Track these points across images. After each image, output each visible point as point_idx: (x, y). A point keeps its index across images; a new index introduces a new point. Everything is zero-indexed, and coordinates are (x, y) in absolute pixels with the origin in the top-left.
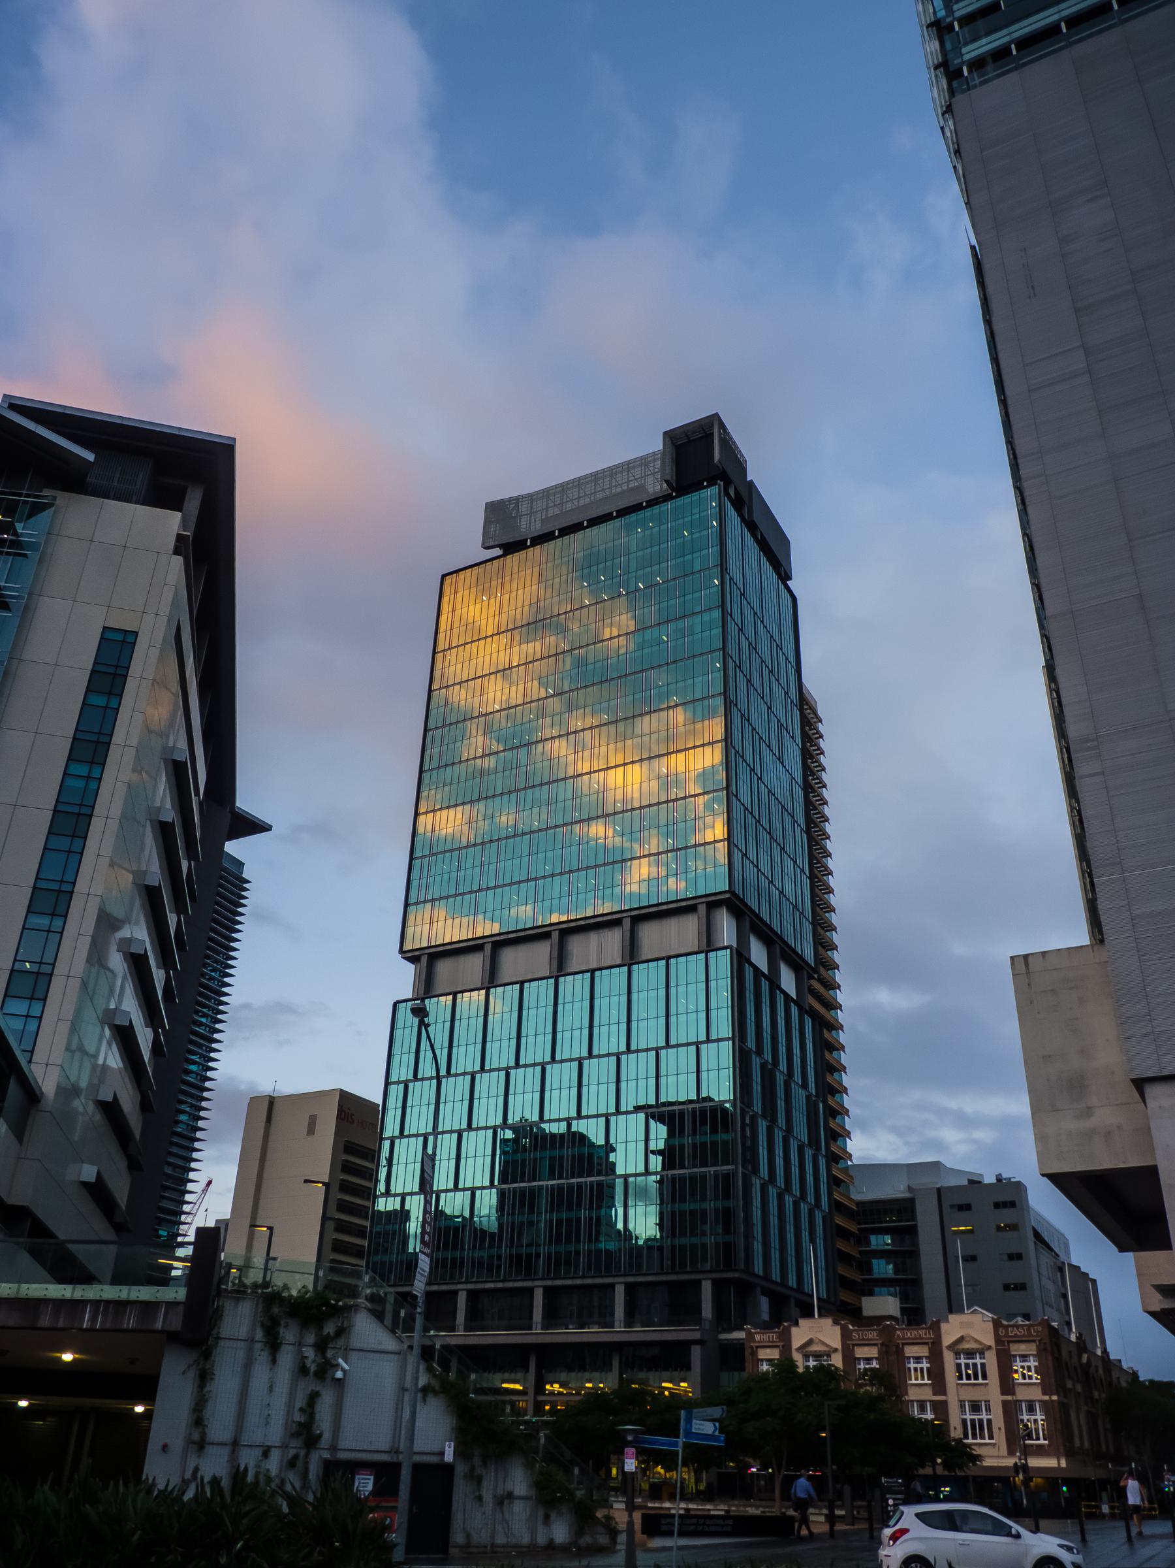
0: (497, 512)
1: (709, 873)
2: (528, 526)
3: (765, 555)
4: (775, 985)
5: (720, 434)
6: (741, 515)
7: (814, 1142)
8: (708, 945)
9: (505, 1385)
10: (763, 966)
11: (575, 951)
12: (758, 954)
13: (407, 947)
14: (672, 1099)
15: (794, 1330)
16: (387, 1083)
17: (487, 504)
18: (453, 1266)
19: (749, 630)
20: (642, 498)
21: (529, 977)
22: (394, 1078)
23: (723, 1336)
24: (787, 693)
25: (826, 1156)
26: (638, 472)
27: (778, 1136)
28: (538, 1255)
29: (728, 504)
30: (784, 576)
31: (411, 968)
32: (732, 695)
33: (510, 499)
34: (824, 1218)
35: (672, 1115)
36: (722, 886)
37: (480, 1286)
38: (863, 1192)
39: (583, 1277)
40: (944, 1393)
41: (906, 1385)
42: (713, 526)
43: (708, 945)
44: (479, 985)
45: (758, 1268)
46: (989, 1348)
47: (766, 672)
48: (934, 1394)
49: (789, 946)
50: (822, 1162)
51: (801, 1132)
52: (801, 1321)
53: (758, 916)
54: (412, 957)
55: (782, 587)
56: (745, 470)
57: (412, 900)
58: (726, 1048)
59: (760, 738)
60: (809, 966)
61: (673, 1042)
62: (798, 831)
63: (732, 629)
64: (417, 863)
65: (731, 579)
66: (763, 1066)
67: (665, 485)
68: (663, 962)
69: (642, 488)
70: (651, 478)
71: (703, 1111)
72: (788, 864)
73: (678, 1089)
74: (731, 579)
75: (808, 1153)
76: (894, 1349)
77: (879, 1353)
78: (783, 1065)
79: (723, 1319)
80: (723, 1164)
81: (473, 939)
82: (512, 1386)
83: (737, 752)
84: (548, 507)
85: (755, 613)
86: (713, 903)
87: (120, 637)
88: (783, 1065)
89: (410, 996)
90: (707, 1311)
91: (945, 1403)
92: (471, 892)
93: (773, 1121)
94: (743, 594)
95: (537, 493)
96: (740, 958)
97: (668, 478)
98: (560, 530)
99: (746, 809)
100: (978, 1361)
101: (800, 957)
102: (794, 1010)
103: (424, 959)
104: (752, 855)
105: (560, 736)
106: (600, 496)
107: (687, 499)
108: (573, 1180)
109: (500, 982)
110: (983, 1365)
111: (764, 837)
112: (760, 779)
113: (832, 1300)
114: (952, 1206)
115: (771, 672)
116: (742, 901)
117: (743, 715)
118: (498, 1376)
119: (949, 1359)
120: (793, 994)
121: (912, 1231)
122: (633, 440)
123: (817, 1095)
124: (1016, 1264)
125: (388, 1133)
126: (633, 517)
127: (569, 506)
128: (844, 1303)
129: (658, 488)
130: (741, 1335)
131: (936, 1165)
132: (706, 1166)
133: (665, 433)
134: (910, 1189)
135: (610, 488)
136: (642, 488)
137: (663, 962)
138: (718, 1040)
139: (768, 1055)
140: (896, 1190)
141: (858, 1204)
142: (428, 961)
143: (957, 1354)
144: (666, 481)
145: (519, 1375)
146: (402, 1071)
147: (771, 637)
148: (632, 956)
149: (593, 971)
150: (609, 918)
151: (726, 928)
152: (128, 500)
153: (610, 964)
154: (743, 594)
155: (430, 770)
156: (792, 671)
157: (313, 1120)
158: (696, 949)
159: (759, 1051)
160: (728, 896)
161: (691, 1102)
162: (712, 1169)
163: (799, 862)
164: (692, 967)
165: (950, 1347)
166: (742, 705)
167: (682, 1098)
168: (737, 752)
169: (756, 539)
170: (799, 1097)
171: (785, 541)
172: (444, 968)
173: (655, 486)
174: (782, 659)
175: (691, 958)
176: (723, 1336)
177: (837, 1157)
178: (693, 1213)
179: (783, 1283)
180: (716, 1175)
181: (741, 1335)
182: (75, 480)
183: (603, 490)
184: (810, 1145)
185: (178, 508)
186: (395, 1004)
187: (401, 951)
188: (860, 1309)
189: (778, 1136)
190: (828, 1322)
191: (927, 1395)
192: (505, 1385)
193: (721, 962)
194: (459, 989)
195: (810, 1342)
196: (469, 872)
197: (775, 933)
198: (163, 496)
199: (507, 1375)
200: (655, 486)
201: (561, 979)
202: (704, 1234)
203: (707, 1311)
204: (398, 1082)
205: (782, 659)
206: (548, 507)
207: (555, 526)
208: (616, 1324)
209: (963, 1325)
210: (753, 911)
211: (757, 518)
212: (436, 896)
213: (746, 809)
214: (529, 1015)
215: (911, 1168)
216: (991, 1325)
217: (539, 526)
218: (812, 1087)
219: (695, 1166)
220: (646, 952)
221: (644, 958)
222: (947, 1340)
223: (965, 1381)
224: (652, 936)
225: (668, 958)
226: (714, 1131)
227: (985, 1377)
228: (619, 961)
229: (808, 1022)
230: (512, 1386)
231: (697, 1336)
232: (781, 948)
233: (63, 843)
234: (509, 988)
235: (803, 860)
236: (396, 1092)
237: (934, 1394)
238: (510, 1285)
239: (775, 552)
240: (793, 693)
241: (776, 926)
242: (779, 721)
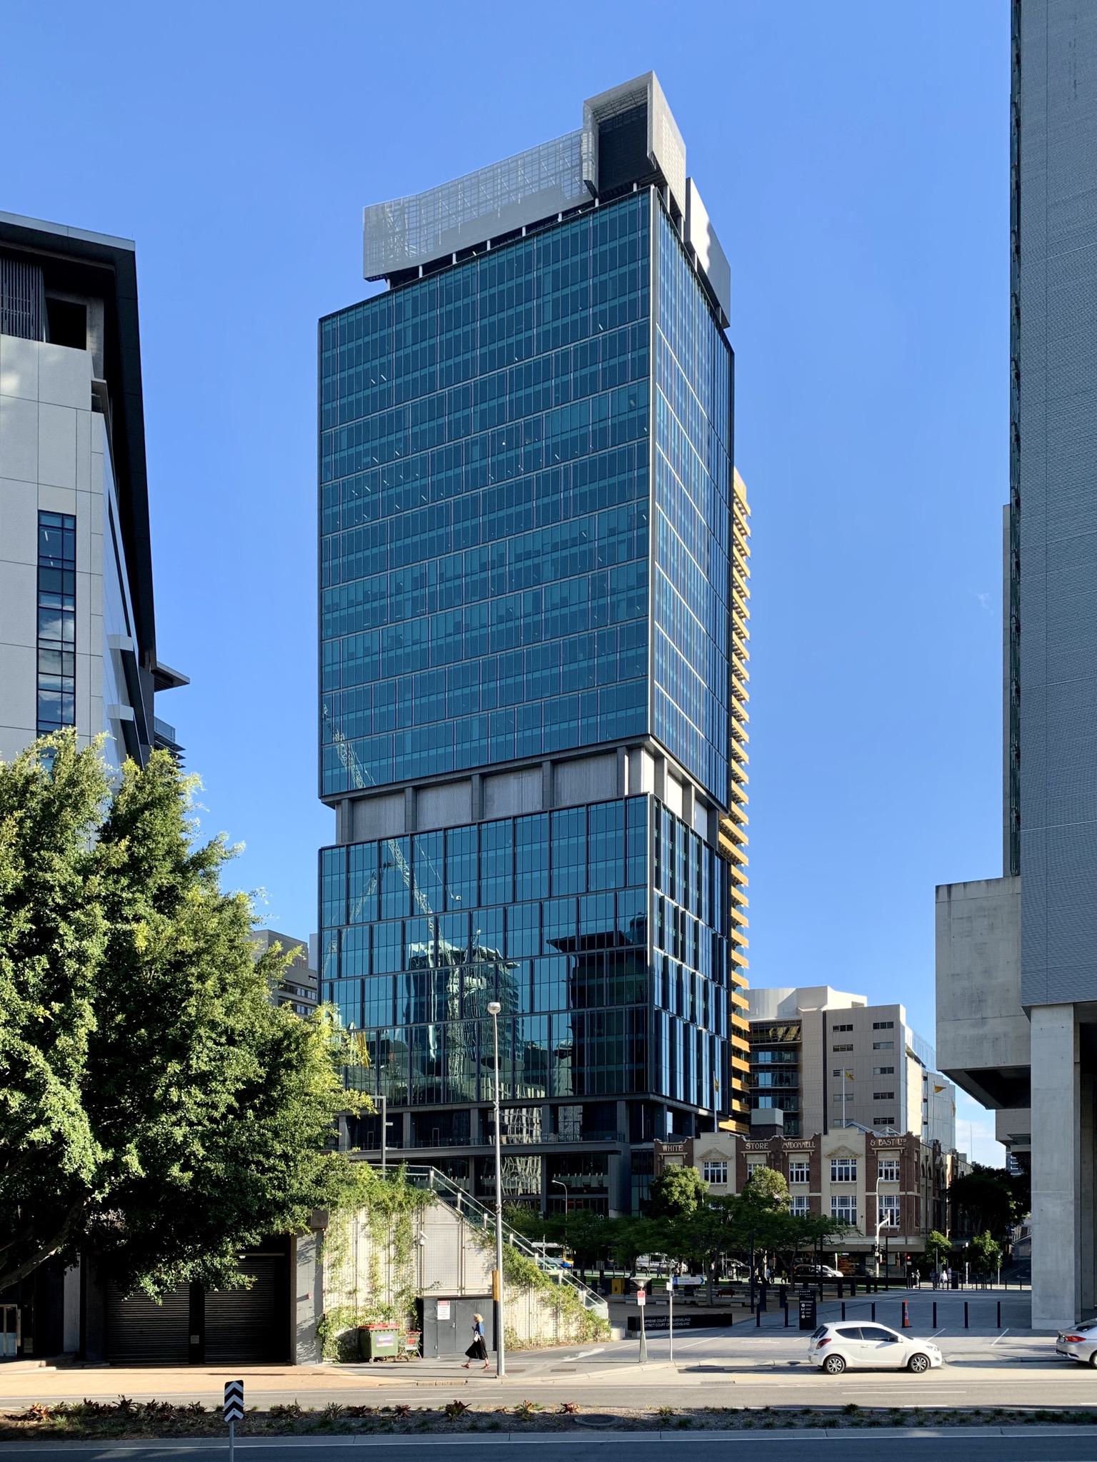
15: (696, 1142)
21: (452, 824)
45: (666, 1091)
50: (723, 993)
52: (702, 1135)
75: (712, 986)
114: (835, 1028)
130: (650, 1145)
172: (366, 811)
181: (650, 1145)
184: (714, 980)
216: (864, 1137)
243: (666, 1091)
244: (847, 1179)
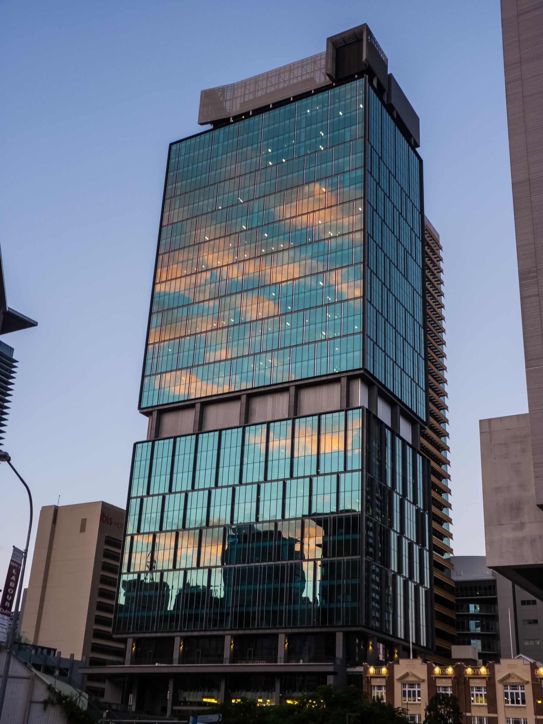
0: (209, 97)
1: (348, 357)
2: (233, 108)
3: (399, 128)
4: (395, 433)
5: (367, 39)
6: (381, 99)
7: (420, 539)
8: (347, 406)
9: (205, 700)
10: (387, 421)
11: (257, 409)
12: (384, 412)
13: (144, 405)
14: (320, 511)
16: (129, 498)
17: (202, 92)
18: (172, 620)
19: (384, 183)
20: (311, 87)
21: (226, 426)
22: (134, 494)
23: (350, 670)
24: (412, 229)
25: (430, 551)
26: (309, 68)
28: (228, 614)
29: (372, 91)
30: (414, 144)
31: (146, 419)
32: (369, 231)
33: (218, 88)
34: (426, 592)
35: (326, 521)
36: (358, 364)
37: (189, 634)
38: (461, 575)
39: (258, 629)
40: (496, 712)
41: (470, 706)
42: (360, 108)
43: (347, 406)
44: (191, 432)
46: (528, 682)
47: (396, 214)
48: (489, 713)
49: (407, 407)
50: (426, 554)
51: (411, 533)
52: (401, 661)
53: (384, 386)
54: (147, 412)
55: (411, 152)
56: (385, 67)
57: (148, 372)
58: (357, 476)
59: (390, 261)
60: (422, 421)
61: (322, 471)
63: (371, 183)
64: (150, 347)
65: (372, 147)
67: (327, 78)
68: (316, 418)
69: (312, 79)
70: (318, 73)
71: (340, 519)
72: (409, 351)
73: (325, 505)
74: (372, 147)
75: (416, 548)
76: (463, 681)
77: (453, 683)
78: (399, 488)
79: (351, 658)
80: (353, 555)
81: (188, 400)
82: (209, 700)
83: (372, 271)
84: (245, 94)
85: (390, 172)
86: (352, 377)
88: (399, 488)
89: (145, 439)
90: (339, 653)
91: (497, 718)
92: (187, 368)
94: (381, 158)
95: (238, 84)
97: (330, 72)
98: (254, 111)
99: (377, 311)
100: (520, 691)
101: (416, 415)
102: (409, 451)
103: (155, 414)
104: (381, 343)
105: (249, 259)
106: (281, 86)
107: (343, 88)
108: (252, 564)
109: (206, 430)
110: (523, 694)
111: (391, 332)
113: (430, 647)
115: (401, 214)
116: (372, 376)
117: (377, 245)
118: (200, 693)
119: (500, 689)
120: (409, 440)
122: (296, 46)
123: (424, 509)
124: (533, 626)
125: (130, 531)
126: (304, 102)
127: (260, 94)
128: (438, 647)
129: (322, 80)
130: (360, 669)
132: (342, 556)
133: (328, 39)
135: (289, 80)
136: (312, 79)
137: (316, 418)
138: (352, 471)
141: (457, 583)
142: (158, 414)
143: (506, 686)
144: (329, 75)
145: (215, 693)
146: (139, 490)
147: (402, 189)
148: (296, 412)
149: (268, 423)
150: (280, 386)
151: (360, 394)
153: (280, 418)
154: (381, 158)
155: (160, 282)
157: (84, 522)
158: (339, 408)
160: (362, 372)
161: (332, 513)
162: (346, 558)
165: (502, 681)
166: (377, 238)
167: (327, 511)
168: (372, 271)
169: (392, 117)
170: (410, 511)
171: (416, 120)
172: (169, 420)
173: (321, 79)
174: (409, 205)
175: (284, 423)
176: (350, 670)
180: (348, 562)
181: (360, 669)
183: (284, 81)
184: (417, 543)
186: (135, 445)
187: (140, 408)
188: (450, 655)
190: (419, 661)
191: (485, 713)
192: (205, 700)
194: (178, 434)
195: (407, 675)
196: (186, 354)
197: (397, 398)
199: (206, 693)
200: (321, 79)
201: (200, 436)
202: (338, 601)
203: (339, 653)
204: (137, 497)
205: (409, 205)
206: (245, 94)
207: (250, 108)
208: (279, 660)
209: (510, 666)
210: (380, 383)
211: (394, 101)
212: (164, 370)
213: (377, 311)
214: (225, 453)
216: (529, 667)
217: (238, 108)
218: (420, 504)
219: (334, 556)
221: (303, 414)
222: (499, 676)
223: (510, 704)
224: (310, 399)
225: (320, 415)
226: (347, 533)
227: (524, 702)
228: (286, 416)
229: (419, 459)
230: (209, 700)
231: (331, 669)
232: (401, 408)
234: (211, 434)
235: (420, 347)
236: (135, 504)
237: (489, 713)
238: (209, 633)
239: (407, 127)
240: (417, 229)
241: (398, 394)
242: (405, 249)
244: (518, 702)
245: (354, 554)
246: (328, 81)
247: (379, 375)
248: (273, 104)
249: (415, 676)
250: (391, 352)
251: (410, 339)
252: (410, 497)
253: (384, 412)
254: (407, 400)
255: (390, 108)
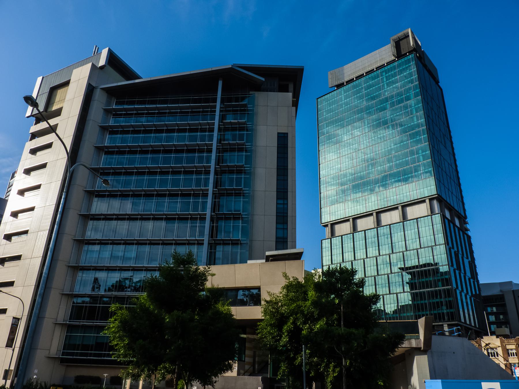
4: (454, 225)
20: (385, 62)
24: (444, 123)
27: (462, 275)
30: (437, 82)
38: (485, 293)
45: (463, 320)
51: (468, 274)
55: (437, 87)
58: (443, 248)
62: (454, 170)
66: (455, 252)
77: (516, 347)
87: (283, 135)
93: (460, 270)
96: (444, 217)
98: (356, 78)
111: (444, 175)
112: (440, 154)
121: (504, 305)
131: (511, 282)
134: (501, 291)
137: (416, 220)
139: (456, 249)
140: (496, 292)
152: (274, 91)
156: (444, 115)
159: (453, 248)
163: (456, 182)
164: (426, 221)
170: (466, 262)
171: (436, 69)
177: (478, 281)
178: (437, 303)
179: (470, 325)
182: (259, 87)
185: (287, 91)
189: (462, 275)
190: (494, 337)
193: (437, 218)
198: (283, 89)
210: (444, 200)
215: (501, 284)
218: (470, 259)
219: (436, 287)
220: (409, 217)
229: (465, 236)
233: (281, 202)
241: (452, 205)
243: (463, 320)
245: (447, 285)
246: (393, 58)
247: (444, 196)
248: (366, 73)
249: (494, 344)
250: (446, 185)
251: (452, 177)
252: (465, 256)
253: (448, 215)
254: (456, 208)
255: (425, 66)
